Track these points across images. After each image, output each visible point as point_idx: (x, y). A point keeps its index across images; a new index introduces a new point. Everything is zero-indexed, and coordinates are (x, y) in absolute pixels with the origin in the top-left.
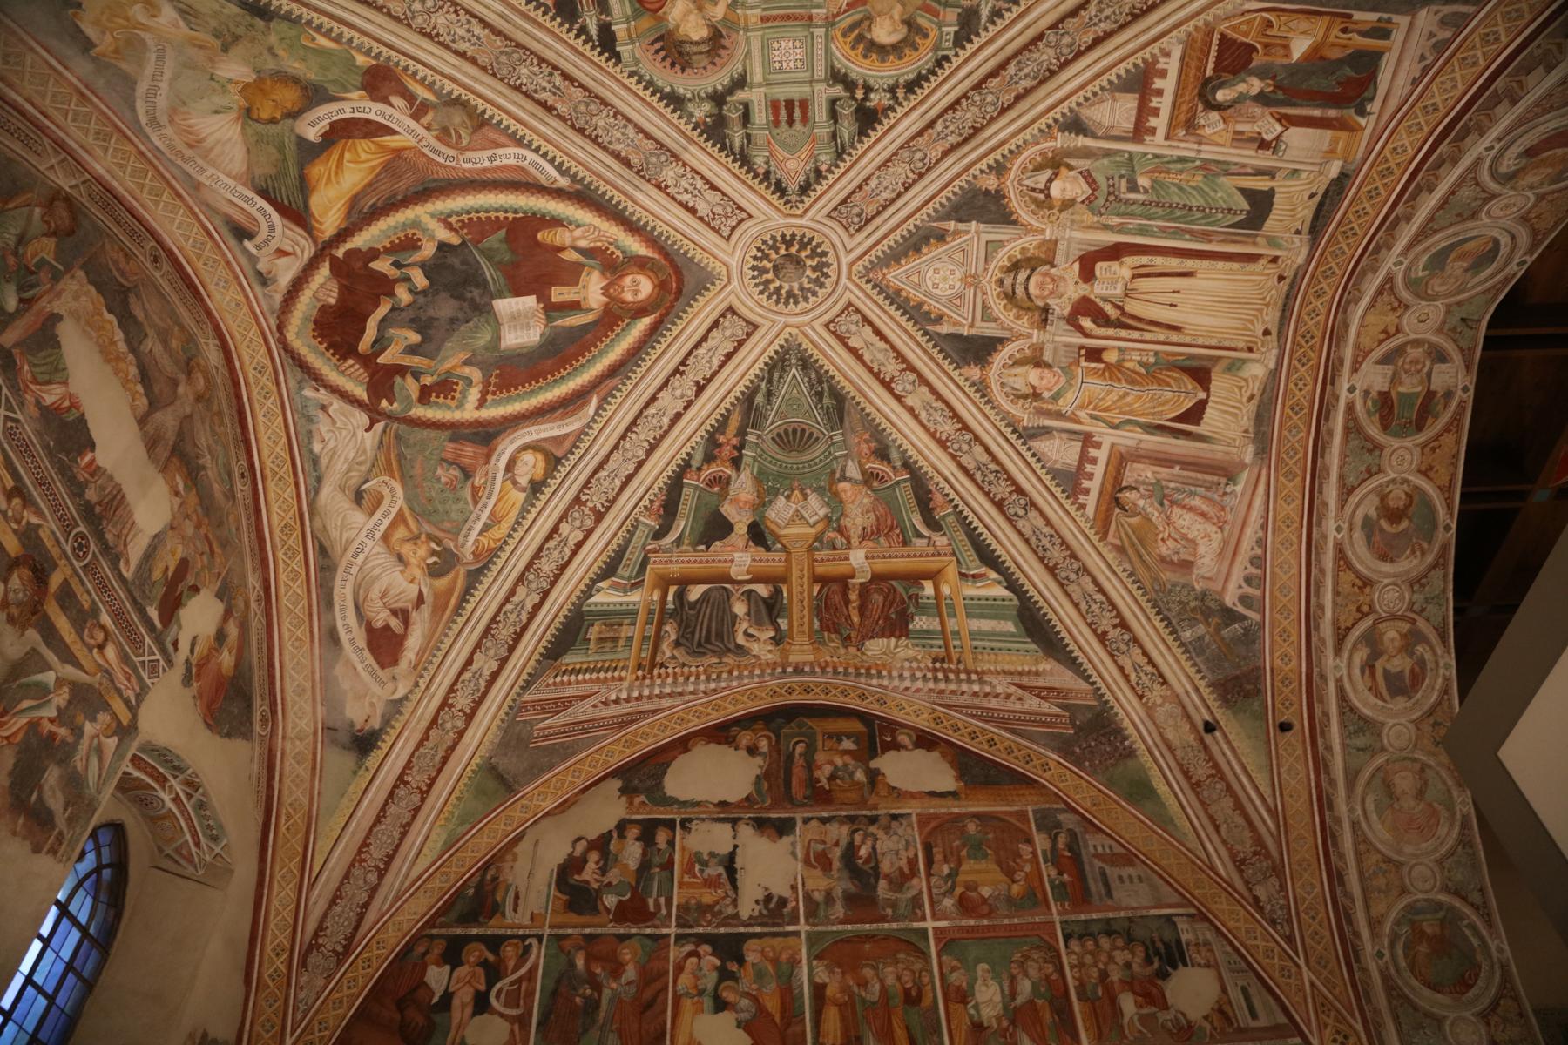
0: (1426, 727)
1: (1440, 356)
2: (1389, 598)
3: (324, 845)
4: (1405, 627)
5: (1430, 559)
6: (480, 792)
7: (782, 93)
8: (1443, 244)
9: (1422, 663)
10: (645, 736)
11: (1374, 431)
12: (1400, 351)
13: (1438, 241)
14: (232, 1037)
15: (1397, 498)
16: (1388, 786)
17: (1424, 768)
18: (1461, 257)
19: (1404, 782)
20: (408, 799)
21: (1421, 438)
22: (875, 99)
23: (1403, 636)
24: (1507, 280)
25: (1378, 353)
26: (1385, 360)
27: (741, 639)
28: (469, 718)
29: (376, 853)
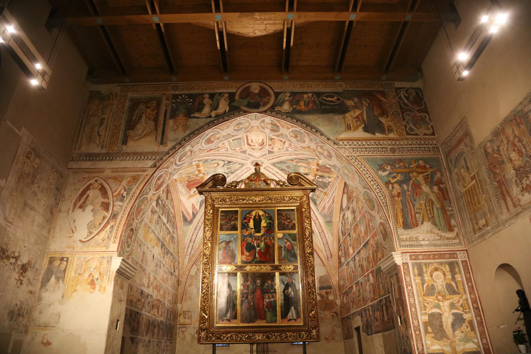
1: (264, 121)
2: (313, 146)
3: (320, 246)
4: (319, 147)
5: (307, 136)
6: (328, 226)
7: (226, 169)
9: (327, 150)
11: (278, 133)
12: (262, 127)
14: (327, 273)
16: (345, 174)
19: (346, 171)
21: (281, 127)
26: (264, 129)
29: (325, 242)
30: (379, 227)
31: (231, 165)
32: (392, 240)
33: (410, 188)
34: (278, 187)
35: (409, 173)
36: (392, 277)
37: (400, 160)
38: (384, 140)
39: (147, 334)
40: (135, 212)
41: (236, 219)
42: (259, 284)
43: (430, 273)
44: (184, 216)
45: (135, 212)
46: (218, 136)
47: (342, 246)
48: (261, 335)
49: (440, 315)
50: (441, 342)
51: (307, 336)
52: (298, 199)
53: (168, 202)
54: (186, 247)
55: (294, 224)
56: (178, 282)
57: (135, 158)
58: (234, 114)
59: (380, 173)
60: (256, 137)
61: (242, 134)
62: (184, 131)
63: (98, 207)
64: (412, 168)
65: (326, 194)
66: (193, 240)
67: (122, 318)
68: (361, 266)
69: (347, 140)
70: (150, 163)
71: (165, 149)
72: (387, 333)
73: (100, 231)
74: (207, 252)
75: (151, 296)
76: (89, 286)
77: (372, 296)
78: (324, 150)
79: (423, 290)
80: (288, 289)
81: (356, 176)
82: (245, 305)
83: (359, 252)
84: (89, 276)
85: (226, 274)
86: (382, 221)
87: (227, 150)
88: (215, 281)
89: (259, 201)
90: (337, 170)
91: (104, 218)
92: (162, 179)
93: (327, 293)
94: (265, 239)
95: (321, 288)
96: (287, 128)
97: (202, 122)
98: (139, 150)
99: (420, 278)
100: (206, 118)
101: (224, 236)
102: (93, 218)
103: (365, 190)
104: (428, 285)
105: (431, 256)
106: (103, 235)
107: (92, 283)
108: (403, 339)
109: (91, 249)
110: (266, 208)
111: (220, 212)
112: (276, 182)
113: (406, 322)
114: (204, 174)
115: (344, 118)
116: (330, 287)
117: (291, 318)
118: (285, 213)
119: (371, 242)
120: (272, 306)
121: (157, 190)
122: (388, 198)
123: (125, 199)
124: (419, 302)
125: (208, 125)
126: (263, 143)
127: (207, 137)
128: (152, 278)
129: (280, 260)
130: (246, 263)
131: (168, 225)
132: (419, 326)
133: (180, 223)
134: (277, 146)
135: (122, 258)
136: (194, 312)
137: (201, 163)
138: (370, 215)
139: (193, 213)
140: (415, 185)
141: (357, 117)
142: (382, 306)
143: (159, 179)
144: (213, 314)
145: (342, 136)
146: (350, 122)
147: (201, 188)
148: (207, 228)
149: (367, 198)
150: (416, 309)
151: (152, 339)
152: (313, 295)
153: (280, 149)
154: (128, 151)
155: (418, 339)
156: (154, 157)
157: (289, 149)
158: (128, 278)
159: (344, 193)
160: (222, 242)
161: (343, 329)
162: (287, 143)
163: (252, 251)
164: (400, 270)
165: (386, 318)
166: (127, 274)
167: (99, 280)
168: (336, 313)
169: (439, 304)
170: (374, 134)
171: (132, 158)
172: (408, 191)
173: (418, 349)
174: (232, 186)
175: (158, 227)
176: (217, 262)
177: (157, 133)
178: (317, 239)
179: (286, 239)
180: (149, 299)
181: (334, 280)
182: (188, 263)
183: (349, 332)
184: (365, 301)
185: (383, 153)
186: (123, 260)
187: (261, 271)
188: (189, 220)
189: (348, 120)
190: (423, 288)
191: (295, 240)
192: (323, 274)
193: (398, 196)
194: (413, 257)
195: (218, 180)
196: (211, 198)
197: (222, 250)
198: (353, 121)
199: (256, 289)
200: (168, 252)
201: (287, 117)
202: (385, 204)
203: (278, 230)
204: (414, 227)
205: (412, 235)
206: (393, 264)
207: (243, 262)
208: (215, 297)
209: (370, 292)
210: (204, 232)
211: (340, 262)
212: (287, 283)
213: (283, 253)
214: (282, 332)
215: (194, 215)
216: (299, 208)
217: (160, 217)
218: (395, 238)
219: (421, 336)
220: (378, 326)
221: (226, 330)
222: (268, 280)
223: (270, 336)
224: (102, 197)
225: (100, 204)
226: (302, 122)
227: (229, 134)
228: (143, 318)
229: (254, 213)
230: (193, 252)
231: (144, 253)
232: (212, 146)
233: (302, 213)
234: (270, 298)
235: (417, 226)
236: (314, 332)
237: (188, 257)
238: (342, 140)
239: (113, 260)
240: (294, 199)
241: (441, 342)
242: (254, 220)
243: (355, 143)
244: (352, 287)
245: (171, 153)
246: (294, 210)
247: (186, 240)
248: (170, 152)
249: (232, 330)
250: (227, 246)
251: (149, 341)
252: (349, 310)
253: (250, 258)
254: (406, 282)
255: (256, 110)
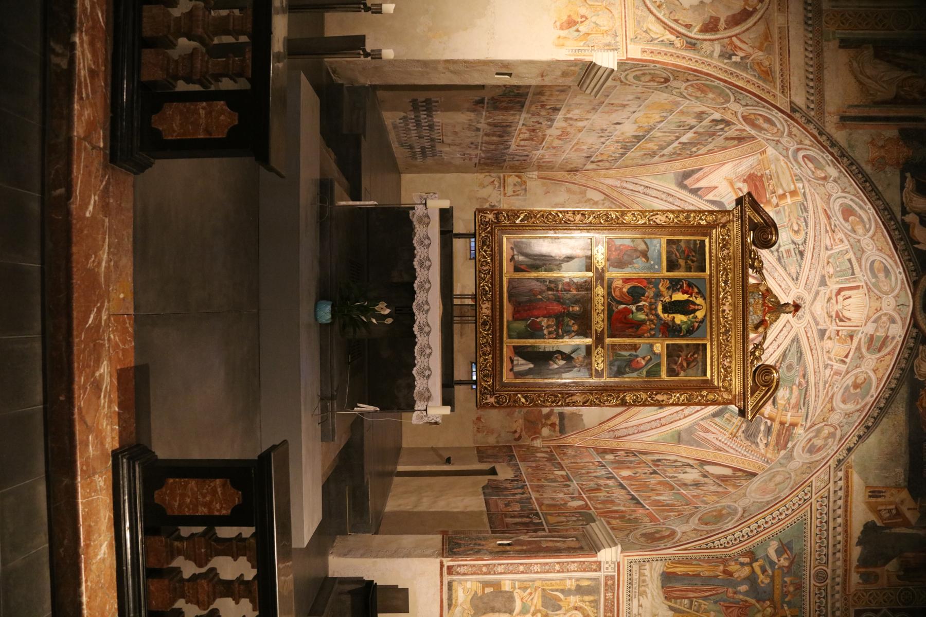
0: (805, 467)
1: (893, 321)
2: (835, 418)
3: (636, 418)
4: (832, 430)
5: (858, 407)
6: (672, 436)
7: (787, 247)
8: (868, 265)
10: (721, 458)
11: (864, 350)
12: (879, 317)
13: (866, 264)
15: (861, 378)
16: (774, 476)
17: (791, 478)
18: (879, 271)
19: (778, 479)
20: (658, 424)
21: (878, 355)
22: (801, 248)
23: (829, 433)
24: (903, 282)
25: (872, 320)
26: (874, 322)
27: (759, 440)
28: (685, 417)
29: (642, 428)
30: (668, 529)
31: (795, 258)
32: (642, 548)
33: (741, 597)
34: (751, 347)
35: (772, 600)
36: (577, 539)
37: (799, 587)
38: (845, 561)
39: (489, 124)
40: (699, 82)
41: (689, 269)
42: (572, 310)
43: (581, 607)
44: (693, 172)
45: (699, 82)
46: (860, 230)
47: (633, 459)
48: (488, 312)
49: (511, 612)
50: (467, 605)
51: (485, 388)
52: (726, 384)
53: (719, 141)
54: (635, 181)
55: (677, 375)
56: (574, 170)
57: (811, 69)
58: (910, 260)
59: (774, 545)
60: (856, 307)
61: (862, 277)
62: (872, 162)
63: (710, 12)
64: (783, 607)
65: (734, 435)
66: (648, 191)
67: (514, 81)
68: (598, 489)
69: (848, 487)
70: (800, 100)
71: (830, 128)
72: (486, 519)
73: (664, 23)
74: (628, 218)
75: (551, 126)
76: (565, 18)
77: (546, 502)
78: (826, 438)
79: (552, 590)
80: (563, 359)
81: (769, 497)
82: (536, 286)
83: (622, 487)
84: (582, 17)
85: (589, 253)
86: (679, 535)
87: (827, 249)
88: (577, 234)
89: (724, 311)
90: (782, 461)
91: (688, 26)
92: (766, 126)
93: (553, 425)
94: (651, 320)
95: (561, 416)
96: (876, 370)
97: (892, 196)
98: (827, 75)
99: (573, 588)
100: (902, 203)
101: (658, 247)
102: (687, 6)
103: (740, 511)
104: (561, 600)
105: (609, 614)
106: (657, 29)
107: (571, 23)
108: (475, 544)
109: (630, 12)
110: (708, 324)
111: (703, 238)
112: (761, 344)
113: (502, 552)
114: (777, 205)
115: (898, 487)
116: (562, 431)
117: (515, 362)
118: (700, 359)
119: (641, 511)
120: (535, 331)
121: (745, 118)
122: (720, 552)
123: (726, 61)
124: (533, 581)
125: (885, 209)
126: (841, 320)
127: (857, 209)
128: (580, 124)
129: (613, 346)
130: (609, 287)
131: (676, 144)
132: (495, 574)
133: (679, 166)
134: (837, 348)
135: (616, 69)
136: (525, 200)
137: (800, 198)
138: (691, 515)
139: (699, 189)
140: (747, 607)
141: (899, 513)
142: (528, 517)
143: (768, 120)
144: (522, 232)
145: (856, 479)
146: (888, 498)
147: (749, 202)
148: (671, 216)
149: (724, 512)
150: (522, 572)
151: (481, 133)
152: (552, 402)
153: (828, 352)
154: (825, 54)
155: (474, 569)
156: (812, 106)
157: (828, 371)
158: (580, 84)
159: (735, 469)
160: (645, 243)
161: (493, 447)
162: (843, 368)
163: (629, 298)
164: (588, 555)
165: (509, 520)
166: (588, 81)
167: (577, 34)
168: (520, 437)
169: (528, 612)
170: (859, 544)
171: (811, 63)
172: (735, 593)
173: (459, 566)
174: (754, 260)
175: (673, 127)
176: (611, 236)
177: (866, 106)
178: (647, 414)
179: (651, 359)
180: (545, 123)
181: (574, 439)
182: (608, 186)
183: (488, 456)
184: (539, 488)
185: (815, 555)
186: (613, 71)
187: (594, 314)
188: (686, 182)
189: (892, 495)
190: (557, 590)
191: (649, 374)
192: (585, 421)
193: (725, 572)
194: (610, 582)
195: (765, 232)
196: (729, 222)
197: (631, 244)
198: (891, 503)
199: (563, 304)
200: (626, 148)
201: (902, 369)
202: (712, 545)
203: (668, 345)
204: (664, 593)
205: (650, 586)
206: (600, 545)
207: (611, 282)
208: (551, 234)
209: (553, 499)
210: (664, 212)
211: (604, 452)
212: (572, 358)
213: (626, 353)
214: (493, 347)
215: (695, 192)
216: (708, 385)
217: (691, 128)
218: (647, 554)
219: (478, 574)
220: (497, 505)
221: (496, 255)
222: (579, 326)
223: (487, 327)
224: (728, 17)
225: (714, 14)
226: (889, 401)
227: (863, 251)
228: (513, 115)
229: (699, 301)
230: (626, 192)
231: (624, 106)
232: (838, 218)
233: (700, 389)
234: (547, 328)
235: (666, 598)
236: (492, 400)
237: (618, 183)
238: (847, 477)
239: (611, 53)
240: (726, 376)
241: (469, 605)
242: (687, 301)
243: (840, 503)
244: (562, 469)
245: (822, 139)
246: (705, 375)
247: (648, 179)
248: (824, 138)
249: (497, 265)
250: (638, 254)
251: (478, 129)
252: (524, 460)
253: (618, 293)
254: (568, 562)
255: (918, 307)
